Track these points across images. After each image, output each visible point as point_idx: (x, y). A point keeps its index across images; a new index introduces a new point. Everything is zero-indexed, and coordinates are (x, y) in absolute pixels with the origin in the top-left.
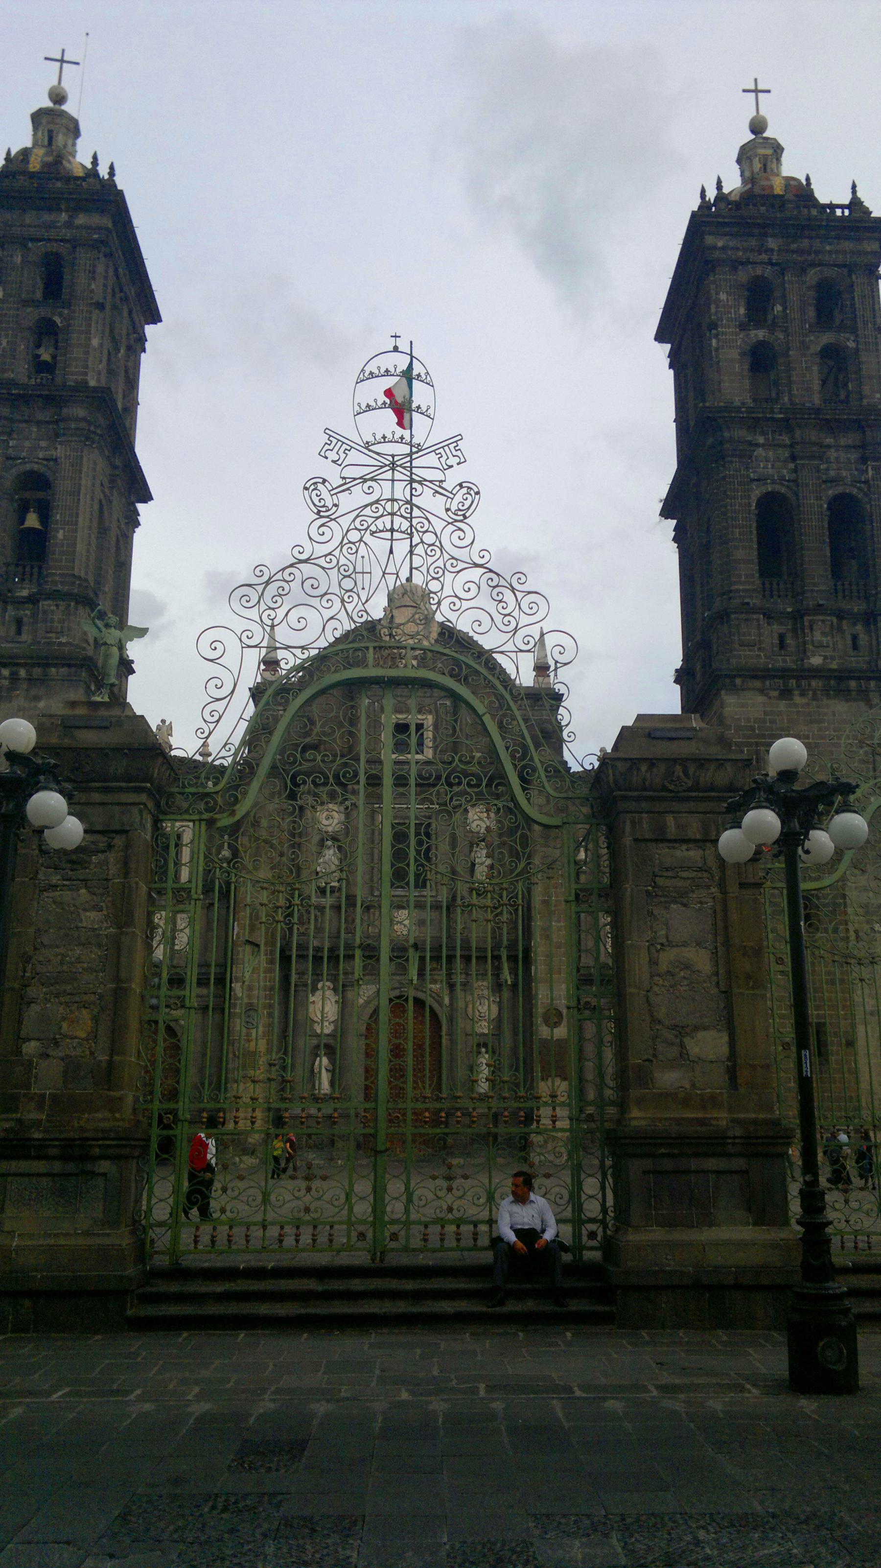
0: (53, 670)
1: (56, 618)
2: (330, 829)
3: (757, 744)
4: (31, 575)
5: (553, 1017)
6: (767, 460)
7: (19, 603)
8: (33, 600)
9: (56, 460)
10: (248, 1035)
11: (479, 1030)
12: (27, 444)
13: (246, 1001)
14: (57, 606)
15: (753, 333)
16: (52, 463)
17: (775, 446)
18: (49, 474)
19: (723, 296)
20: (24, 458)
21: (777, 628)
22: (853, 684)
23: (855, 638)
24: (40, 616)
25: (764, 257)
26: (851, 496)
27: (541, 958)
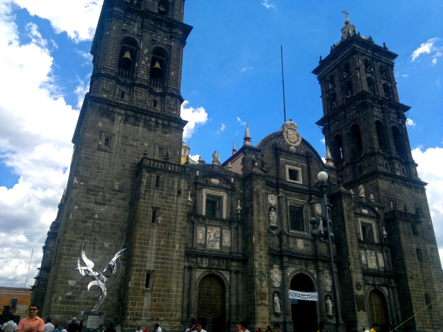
0: (172, 123)
1: (172, 104)
2: (273, 204)
3: (388, 197)
4: (160, 85)
5: (359, 286)
6: (376, 111)
7: (156, 94)
8: (162, 95)
9: (171, 46)
10: (261, 285)
11: (327, 290)
12: (159, 37)
13: (259, 270)
14: (172, 99)
15: (368, 74)
16: (169, 47)
17: (378, 108)
18: (167, 50)
19: (360, 61)
20: (159, 42)
21: (385, 162)
22: (408, 183)
23: (403, 169)
24: (166, 101)
25: (368, 54)
26: (396, 127)
27: (352, 263)
